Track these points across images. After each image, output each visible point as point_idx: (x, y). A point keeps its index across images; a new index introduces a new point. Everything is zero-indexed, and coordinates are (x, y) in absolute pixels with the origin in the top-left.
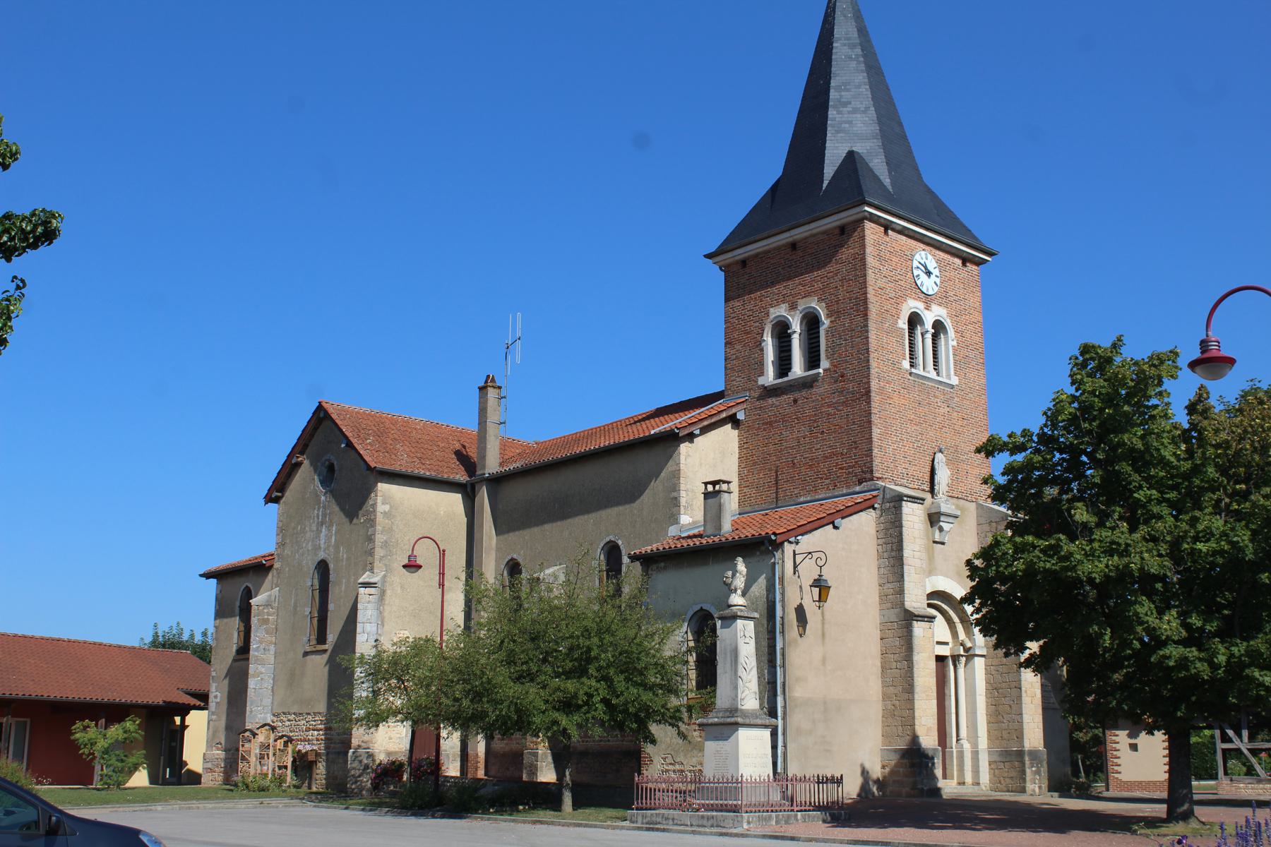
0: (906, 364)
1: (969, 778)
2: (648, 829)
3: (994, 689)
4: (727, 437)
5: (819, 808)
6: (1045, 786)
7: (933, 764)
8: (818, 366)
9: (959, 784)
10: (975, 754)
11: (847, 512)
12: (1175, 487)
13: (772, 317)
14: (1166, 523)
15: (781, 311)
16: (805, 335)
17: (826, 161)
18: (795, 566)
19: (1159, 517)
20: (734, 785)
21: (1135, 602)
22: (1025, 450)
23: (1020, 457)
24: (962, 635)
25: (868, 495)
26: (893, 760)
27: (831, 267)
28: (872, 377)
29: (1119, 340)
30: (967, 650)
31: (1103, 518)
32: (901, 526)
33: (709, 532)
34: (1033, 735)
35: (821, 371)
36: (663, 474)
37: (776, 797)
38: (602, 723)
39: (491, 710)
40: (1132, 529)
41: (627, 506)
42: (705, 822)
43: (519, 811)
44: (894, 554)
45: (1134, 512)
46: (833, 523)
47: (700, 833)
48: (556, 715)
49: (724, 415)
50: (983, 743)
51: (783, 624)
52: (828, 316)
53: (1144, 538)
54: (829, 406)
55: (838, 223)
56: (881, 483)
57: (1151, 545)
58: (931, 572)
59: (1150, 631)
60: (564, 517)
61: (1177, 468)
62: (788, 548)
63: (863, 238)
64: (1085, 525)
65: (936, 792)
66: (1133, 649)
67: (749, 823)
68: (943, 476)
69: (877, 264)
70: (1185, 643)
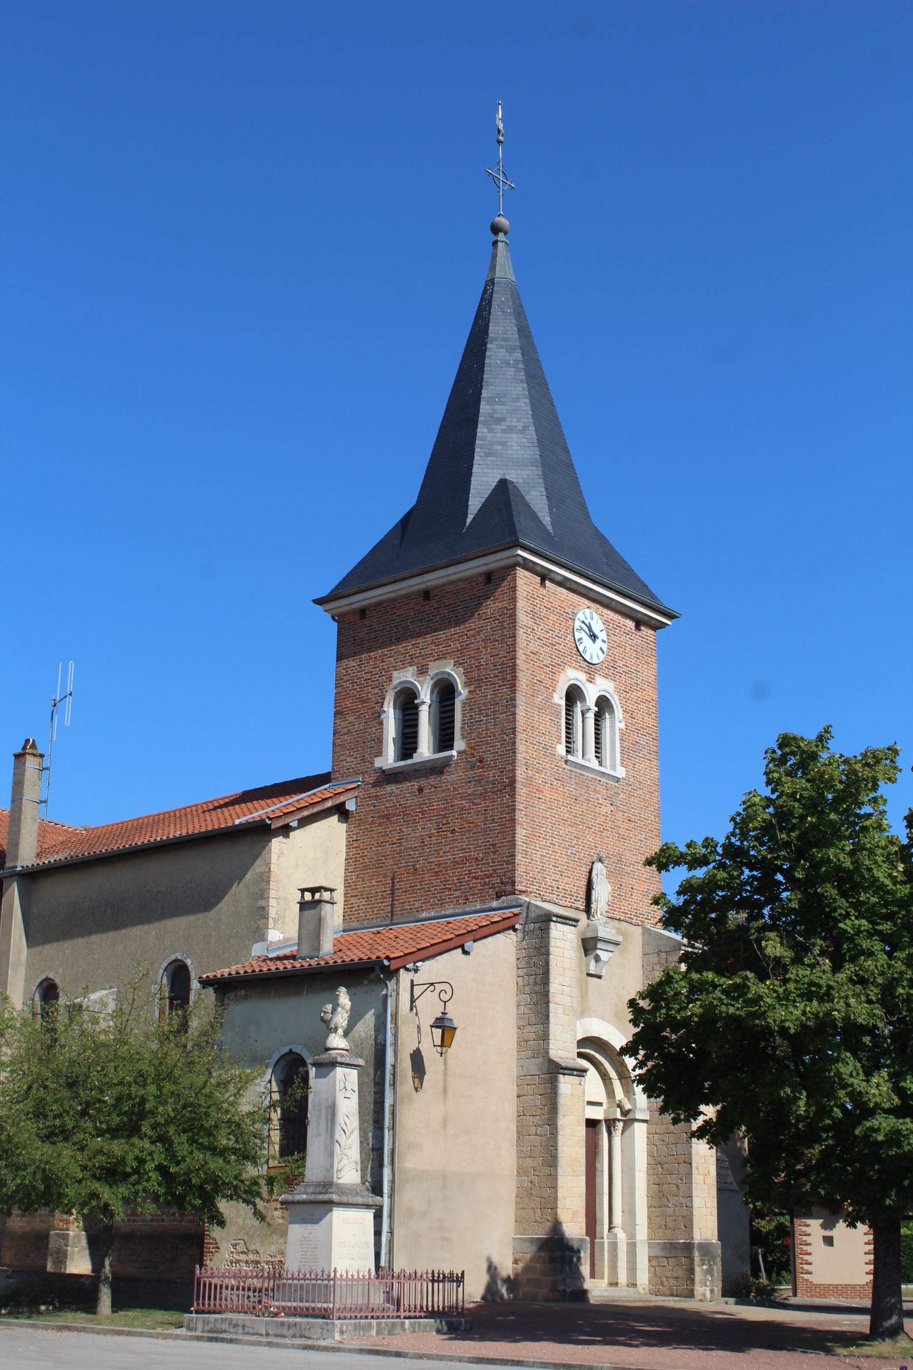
0: (561, 749)
1: (623, 1278)
2: (211, 1339)
3: (657, 1163)
4: (333, 830)
5: (432, 1314)
6: (718, 1289)
7: (579, 1259)
8: (451, 747)
9: (611, 1284)
10: (632, 1247)
11: (481, 933)
12: (889, 917)
13: (395, 682)
14: (877, 962)
15: (406, 675)
16: (436, 706)
17: (472, 491)
18: (413, 1001)
19: (870, 954)
20: (324, 1283)
21: (837, 1060)
22: (707, 863)
23: (700, 873)
24: (619, 1094)
25: (508, 913)
26: (529, 1252)
27: (473, 624)
28: (518, 764)
29: (827, 731)
30: (625, 1113)
31: (800, 952)
32: (547, 954)
33: (304, 953)
34: (705, 1225)
35: (454, 753)
36: (248, 877)
37: (378, 1299)
38: (156, 1198)
39: (9, 1177)
40: (837, 968)
41: (201, 916)
42: (284, 1331)
43: (39, 1313)
44: (537, 988)
45: (838, 947)
46: (462, 946)
47: (277, 1345)
48: (96, 1186)
49: (329, 804)
50: (642, 1232)
51: (394, 1075)
52: (466, 685)
53: (850, 980)
54: (463, 798)
55: (483, 569)
56: (524, 898)
57: (859, 988)
58: (583, 1012)
59: (856, 1096)
60: (117, 926)
61: (893, 893)
62: (405, 977)
63: (514, 589)
64: (778, 960)
65: (582, 1294)
66: (833, 1119)
67: (342, 1332)
68: (602, 892)
69: (531, 623)
70: (898, 1112)
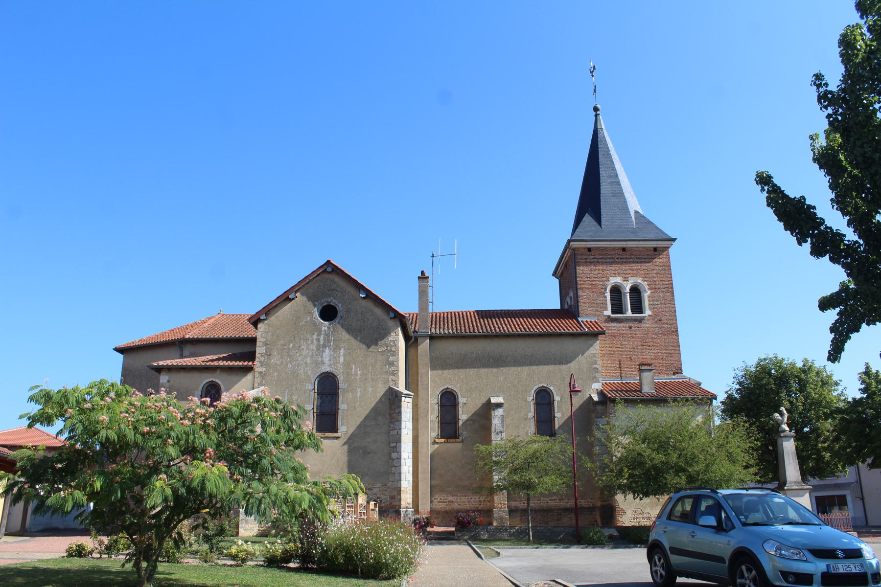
60: (498, 366)
